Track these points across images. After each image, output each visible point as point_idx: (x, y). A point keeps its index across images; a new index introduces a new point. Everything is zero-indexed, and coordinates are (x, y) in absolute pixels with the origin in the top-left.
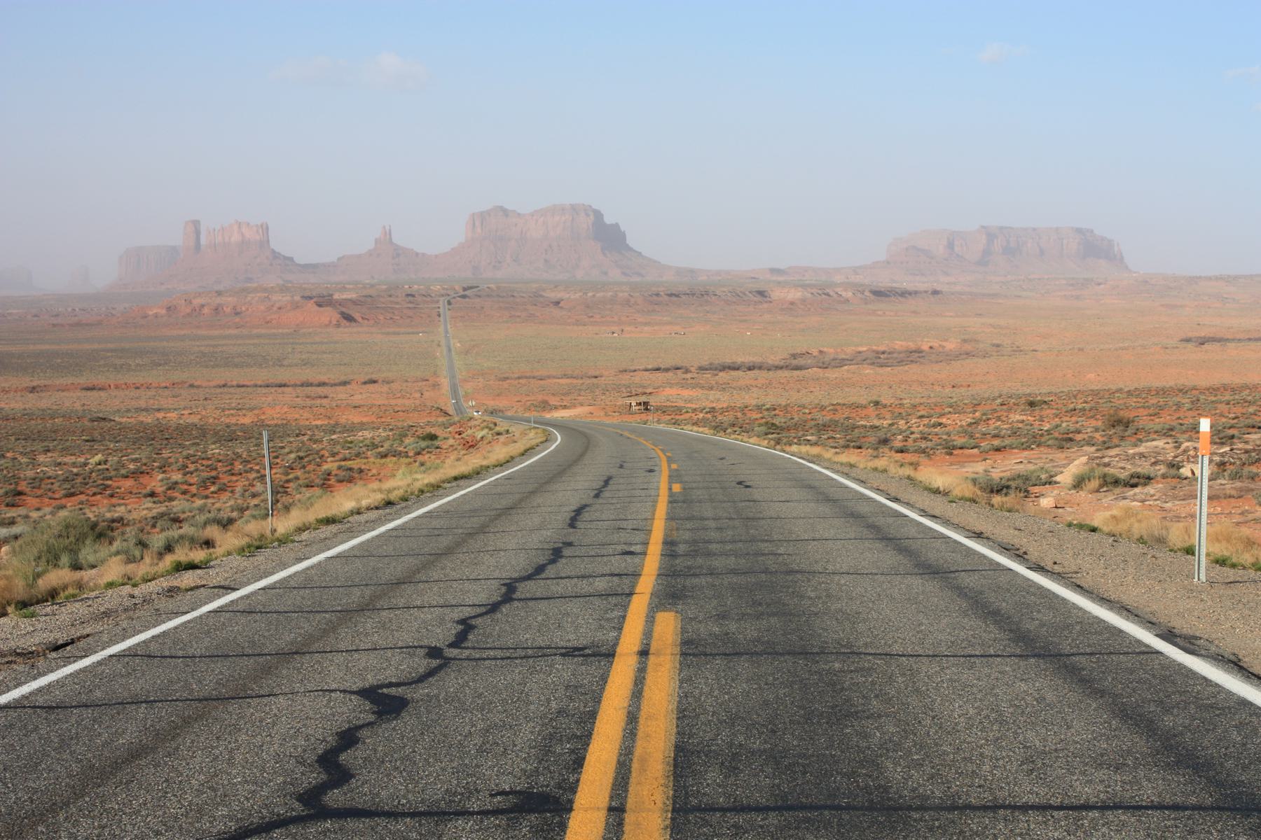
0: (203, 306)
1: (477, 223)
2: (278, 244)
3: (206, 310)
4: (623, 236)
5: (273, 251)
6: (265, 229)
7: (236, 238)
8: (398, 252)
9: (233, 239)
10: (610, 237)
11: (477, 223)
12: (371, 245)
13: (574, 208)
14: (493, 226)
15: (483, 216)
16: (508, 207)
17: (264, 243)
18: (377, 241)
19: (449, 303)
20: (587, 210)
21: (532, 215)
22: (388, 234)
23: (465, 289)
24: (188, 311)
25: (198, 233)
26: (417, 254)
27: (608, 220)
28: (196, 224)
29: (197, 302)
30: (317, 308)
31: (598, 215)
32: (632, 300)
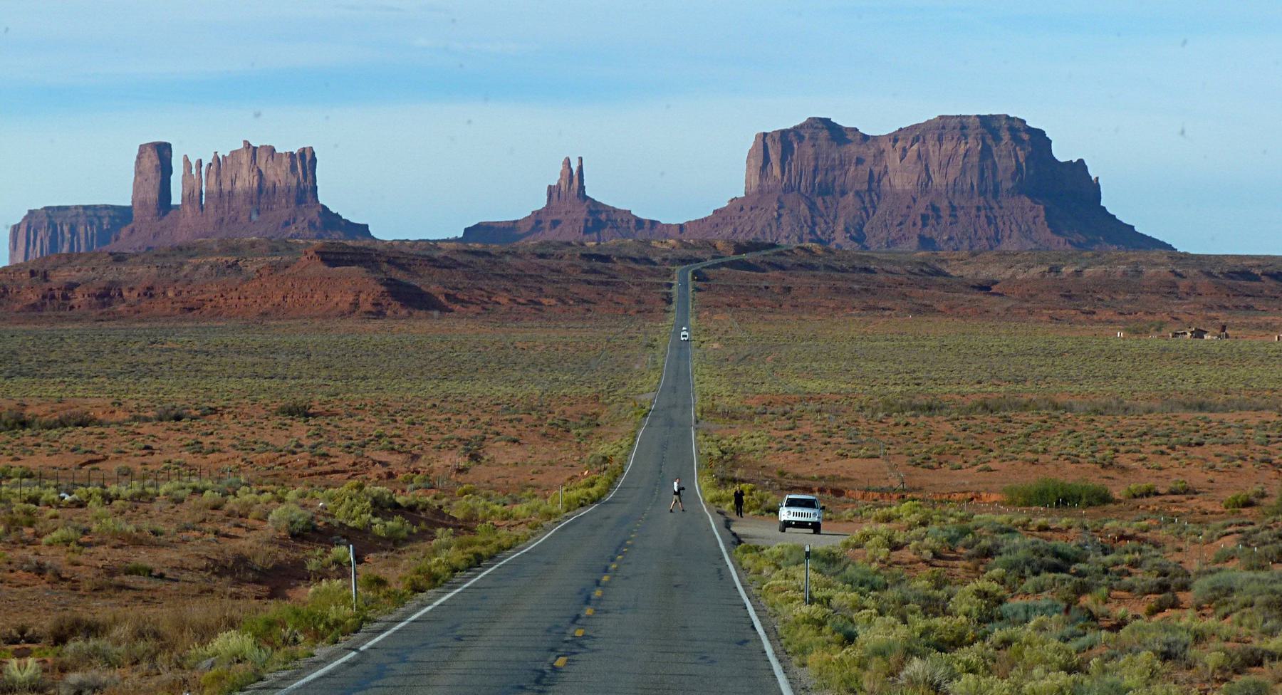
0: (71, 287)
1: (774, 157)
2: (337, 193)
3: (78, 298)
4: (1094, 189)
5: (324, 207)
6: (306, 161)
7: (245, 180)
8: (601, 217)
9: (239, 184)
10: (1068, 194)
11: (774, 157)
12: (541, 202)
13: (988, 124)
14: (807, 159)
15: (787, 140)
16: (843, 121)
17: (306, 191)
18: (550, 187)
19: (699, 276)
20: (1016, 127)
21: (894, 138)
22: (574, 178)
23: (740, 249)
24: (33, 297)
25: (165, 169)
26: (640, 222)
27: (1061, 153)
28: (162, 151)
29: (61, 276)
30: (323, 267)
31: (1040, 140)
32: (1183, 284)
